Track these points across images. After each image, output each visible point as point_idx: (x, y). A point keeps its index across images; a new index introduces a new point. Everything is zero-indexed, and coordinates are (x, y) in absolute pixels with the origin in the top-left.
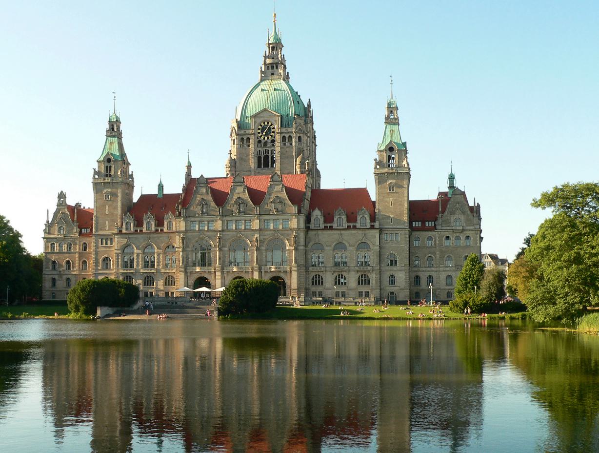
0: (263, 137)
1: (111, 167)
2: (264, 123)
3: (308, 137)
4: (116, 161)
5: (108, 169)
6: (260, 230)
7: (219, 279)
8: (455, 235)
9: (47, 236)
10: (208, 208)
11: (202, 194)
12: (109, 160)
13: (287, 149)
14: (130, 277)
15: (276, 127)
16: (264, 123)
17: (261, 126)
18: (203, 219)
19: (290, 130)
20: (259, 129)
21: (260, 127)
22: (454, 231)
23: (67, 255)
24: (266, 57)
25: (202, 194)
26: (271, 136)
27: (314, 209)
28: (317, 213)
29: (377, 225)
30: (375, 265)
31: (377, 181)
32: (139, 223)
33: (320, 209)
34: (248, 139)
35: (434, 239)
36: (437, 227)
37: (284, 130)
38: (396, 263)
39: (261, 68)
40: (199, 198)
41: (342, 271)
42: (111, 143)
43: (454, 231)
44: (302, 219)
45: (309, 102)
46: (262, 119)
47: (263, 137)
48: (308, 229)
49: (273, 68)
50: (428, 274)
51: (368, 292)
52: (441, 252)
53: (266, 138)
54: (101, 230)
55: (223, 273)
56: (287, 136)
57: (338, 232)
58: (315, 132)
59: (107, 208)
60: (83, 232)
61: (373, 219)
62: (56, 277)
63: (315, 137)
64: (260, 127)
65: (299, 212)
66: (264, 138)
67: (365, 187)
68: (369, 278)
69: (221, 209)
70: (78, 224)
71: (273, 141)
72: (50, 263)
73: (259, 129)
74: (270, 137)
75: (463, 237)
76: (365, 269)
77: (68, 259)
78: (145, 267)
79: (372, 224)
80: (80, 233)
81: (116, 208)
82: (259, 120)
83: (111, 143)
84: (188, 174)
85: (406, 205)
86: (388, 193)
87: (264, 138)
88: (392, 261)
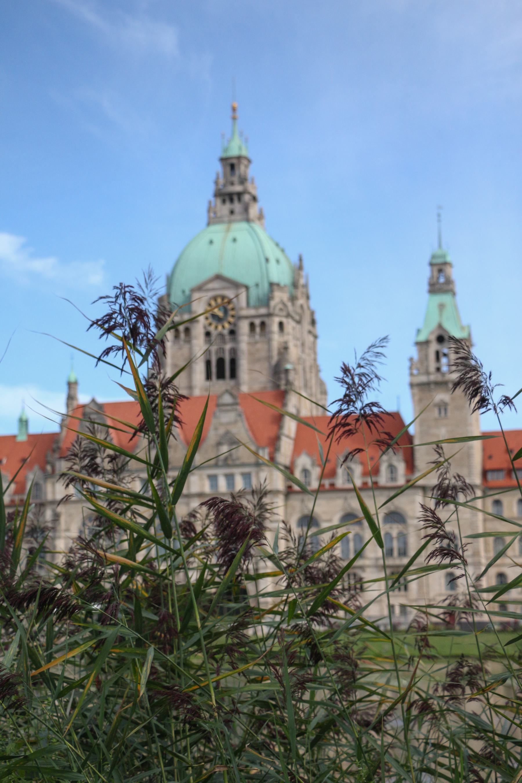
3: (299, 322)
13: (259, 346)
24: (216, 183)
26: (229, 323)
31: (417, 398)
33: (310, 454)
39: (210, 202)
45: (301, 260)
48: (289, 492)
49: (232, 201)
56: (257, 322)
58: (312, 313)
63: (313, 322)
66: (216, 328)
71: (232, 332)
74: (227, 325)
82: (206, 296)
84: (71, 398)
86: (436, 420)
87: (216, 328)
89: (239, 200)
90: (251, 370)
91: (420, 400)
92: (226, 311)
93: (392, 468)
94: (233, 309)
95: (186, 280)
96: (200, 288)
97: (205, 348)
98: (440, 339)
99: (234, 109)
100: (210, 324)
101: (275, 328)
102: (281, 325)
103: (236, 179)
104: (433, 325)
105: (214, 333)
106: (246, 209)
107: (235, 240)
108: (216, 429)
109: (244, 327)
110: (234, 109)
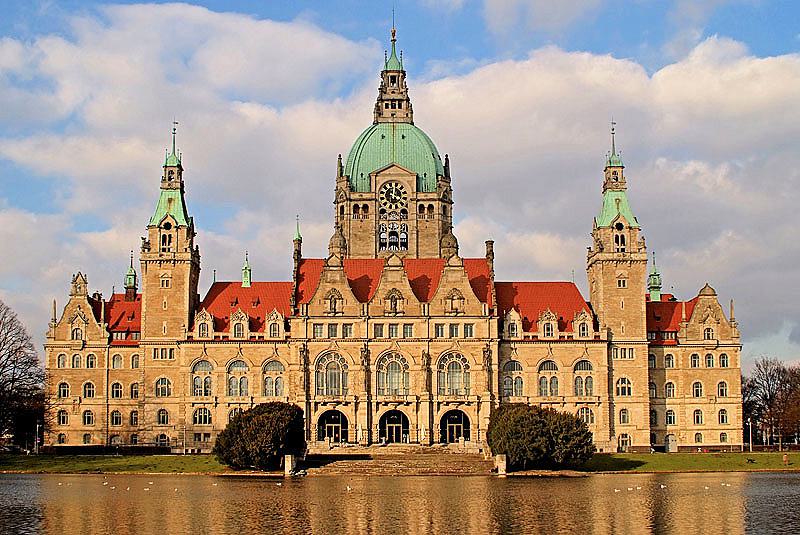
0: (388, 205)
2: (391, 185)
4: (177, 228)
9: (51, 342)
11: (334, 282)
12: (168, 226)
14: (205, 409)
15: (409, 192)
16: (391, 185)
17: (386, 188)
18: (335, 321)
19: (430, 196)
20: (382, 193)
21: (383, 190)
25: (334, 282)
26: (402, 204)
28: (514, 317)
29: (603, 336)
30: (601, 395)
32: (220, 325)
34: (365, 207)
36: (680, 340)
37: (421, 196)
38: (629, 394)
40: (329, 287)
42: (170, 200)
44: (494, 322)
45: (447, 159)
46: (389, 178)
47: (388, 205)
49: (393, 107)
52: (687, 376)
53: (394, 206)
54: (154, 334)
55: (369, 404)
56: (426, 206)
57: (547, 345)
59: (165, 298)
60: (114, 338)
61: (596, 327)
62: (69, 408)
64: (383, 190)
65: (491, 311)
66: (391, 207)
68: (592, 414)
69: (366, 306)
70: (106, 324)
73: (382, 193)
74: (399, 205)
75: (716, 356)
78: (195, 394)
79: (597, 334)
80: (110, 339)
81: (180, 301)
82: (381, 180)
83: (170, 200)
84: (298, 252)
85: (644, 308)
87: (391, 207)
88: (623, 388)
89: (400, 107)
94: (405, 193)
95: (368, 165)
99: (394, 34)
100: (385, 204)
101: (441, 212)
110: (394, 34)
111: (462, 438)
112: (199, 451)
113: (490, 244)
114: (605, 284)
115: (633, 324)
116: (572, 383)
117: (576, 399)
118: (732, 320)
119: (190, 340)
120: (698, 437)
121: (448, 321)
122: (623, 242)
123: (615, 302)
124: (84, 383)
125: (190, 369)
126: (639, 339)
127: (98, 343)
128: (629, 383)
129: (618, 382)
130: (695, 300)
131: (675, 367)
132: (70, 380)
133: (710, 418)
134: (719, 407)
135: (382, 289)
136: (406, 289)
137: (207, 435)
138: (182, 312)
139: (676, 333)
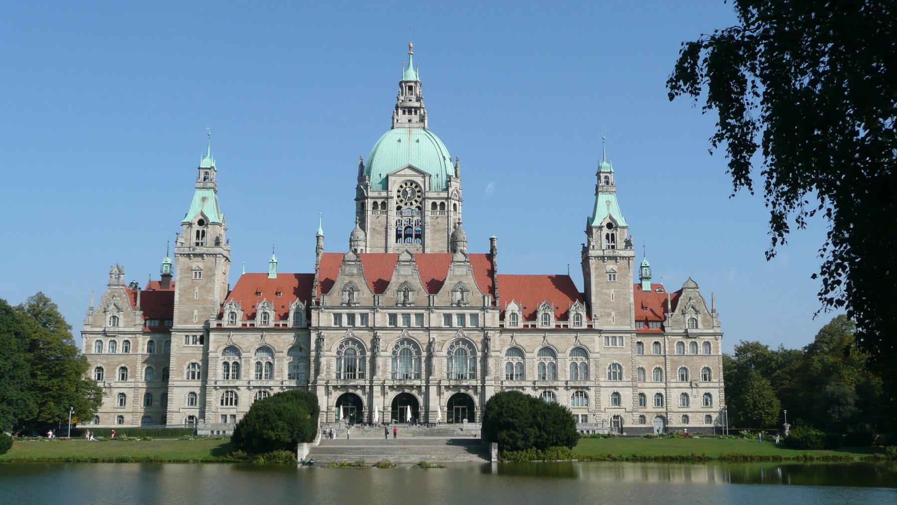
0: (404, 203)
1: (203, 232)
5: (200, 235)
6: (439, 329)
7: (378, 397)
8: (690, 340)
9: (88, 329)
10: (361, 296)
11: (352, 275)
13: (439, 220)
14: (232, 392)
18: (353, 311)
22: (687, 335)
23: (121, 359)
26: (416, 201)
27: (509, 302)
28: (512, 307)
33: (517, 302)
34: (384, 205)
35: (662, 345)
36: (666, 329)
40: (347, 280)
41: (549, 387)
43: (687, 335)
47: (404, 203)
49: (410, 112)
50: (656, 391)
51: (586, 416)
52: (673, 362)
54: (186, 322)
56: (438, 202)
59: (197, 290)
65: (494, 303)
66: (406, 204)
67: (564, 273)
72: (93, 371)
74: (414, 203)
76: (582, 385)
77: (123, 365)
81: (211, 291)
84: (318, 248)
85: (632, 300)
87: (406, 204)
88: (615, 373)
90: (433, 239)
91: (596, 268)
92: (413, 193)
93: (578, 317)
96: (394, 174)
97: (397, 218)
98: (609, 226)
100: (401, 201)
102: (455, 205)
103: (414, 98)
104: (606, 214)
105: (404, 208)
106: (422, 120)
107: (418, 141)
108: (451, 279)
109: (428, 204)
111: (466, 420)
112: (224, 432)
113: (492, 240)
114: (597, 277)
115: (622, 314)
116: (568, 369)
117: (571, 384)
118: (713, 311)
119: (219, 328)
120: (686, 418)
121: (454, 312)
122: (613, 239)
123: (606, 294)
124: (118, 368)
125: (219, 354)
126: (628, 328)
127: (133, 329)
128: (620, 367)
129: (610, 368)
130: (680, 293)
131: (662, 353)
132: (104, 364)
133: (697, 402)
134: (702, 392)
135: (395, 282)
136: (417, 282)
137: (234, 416)
138: (214, 303)
139: (662, 322)
